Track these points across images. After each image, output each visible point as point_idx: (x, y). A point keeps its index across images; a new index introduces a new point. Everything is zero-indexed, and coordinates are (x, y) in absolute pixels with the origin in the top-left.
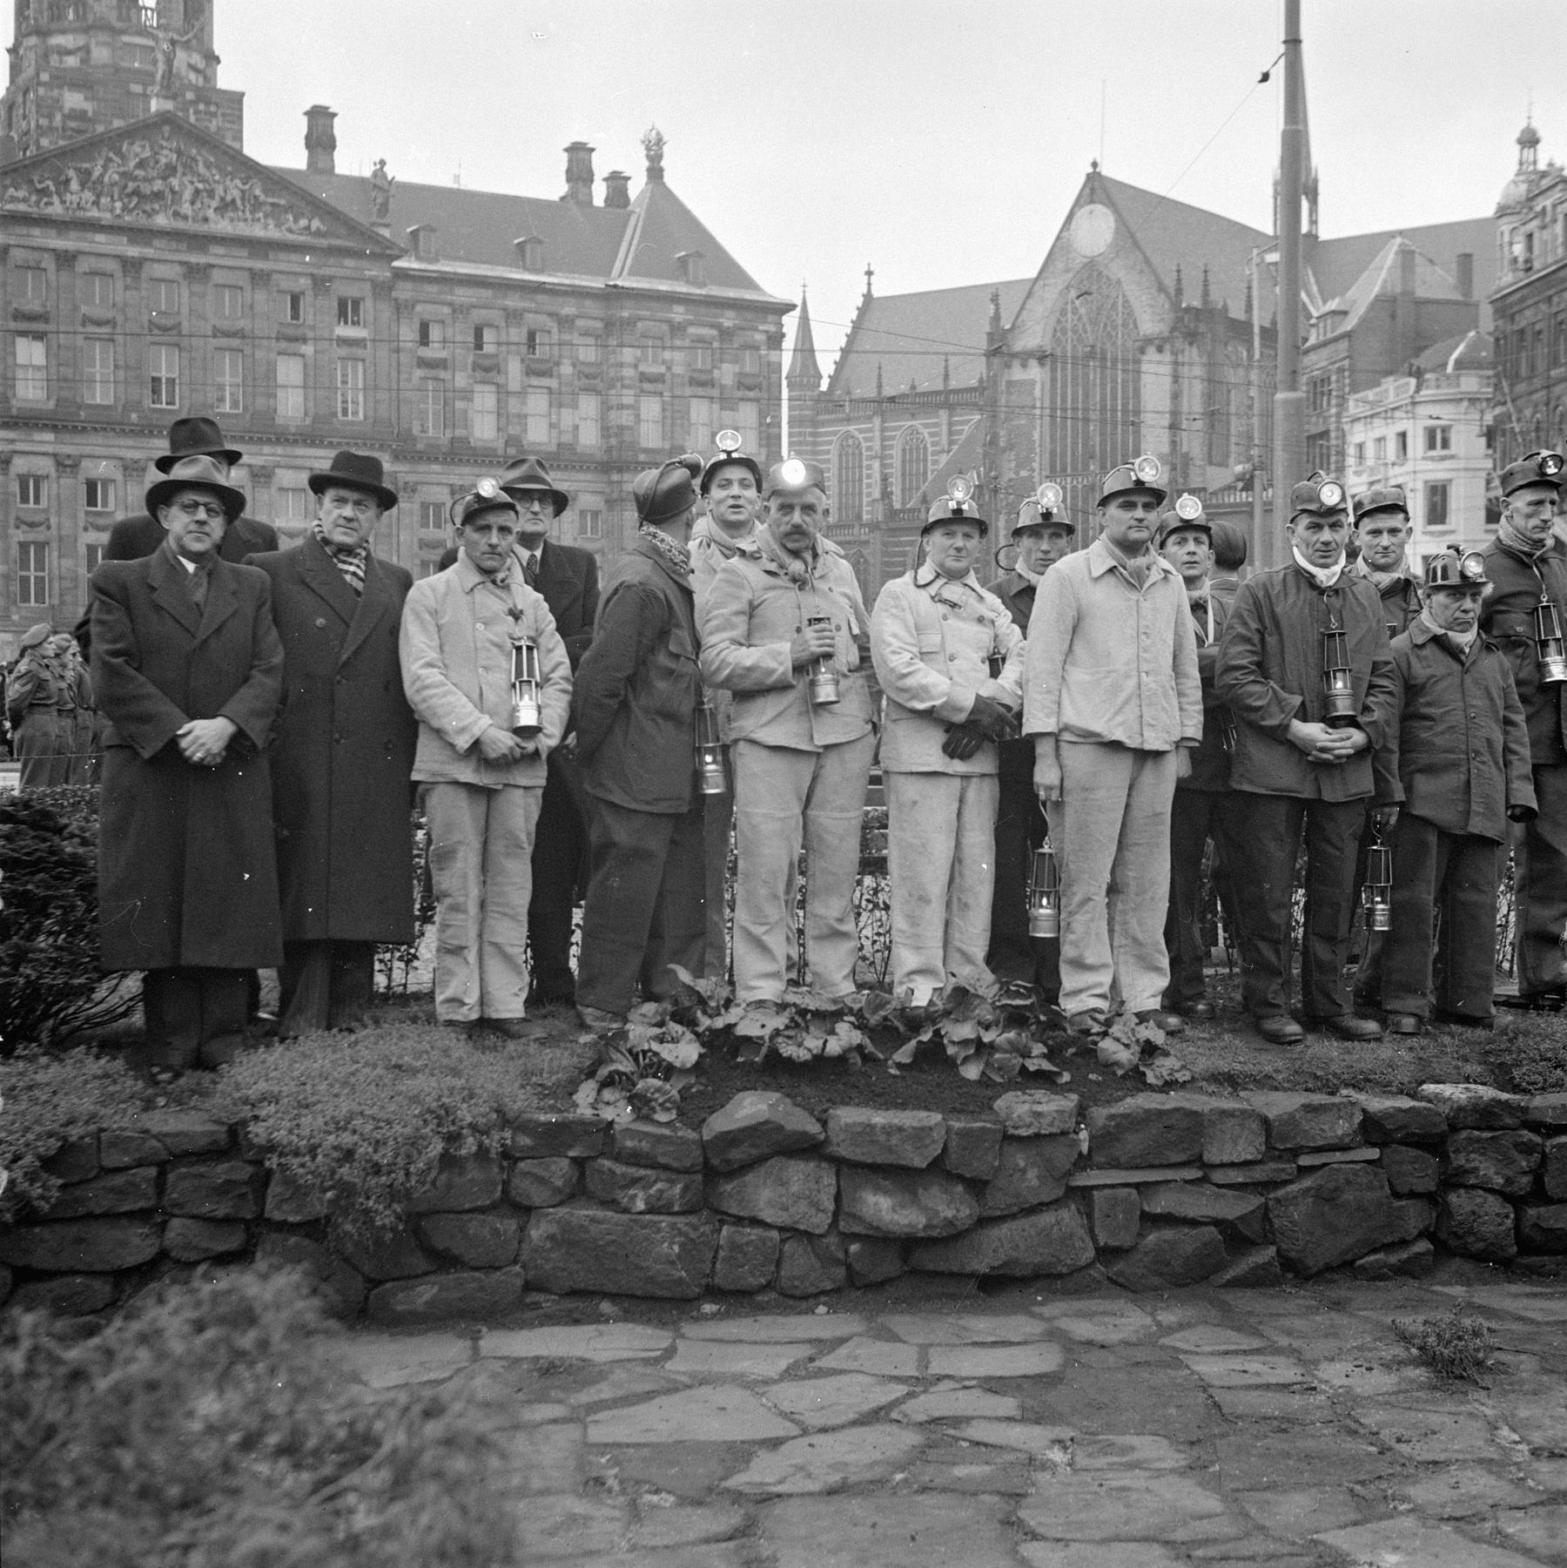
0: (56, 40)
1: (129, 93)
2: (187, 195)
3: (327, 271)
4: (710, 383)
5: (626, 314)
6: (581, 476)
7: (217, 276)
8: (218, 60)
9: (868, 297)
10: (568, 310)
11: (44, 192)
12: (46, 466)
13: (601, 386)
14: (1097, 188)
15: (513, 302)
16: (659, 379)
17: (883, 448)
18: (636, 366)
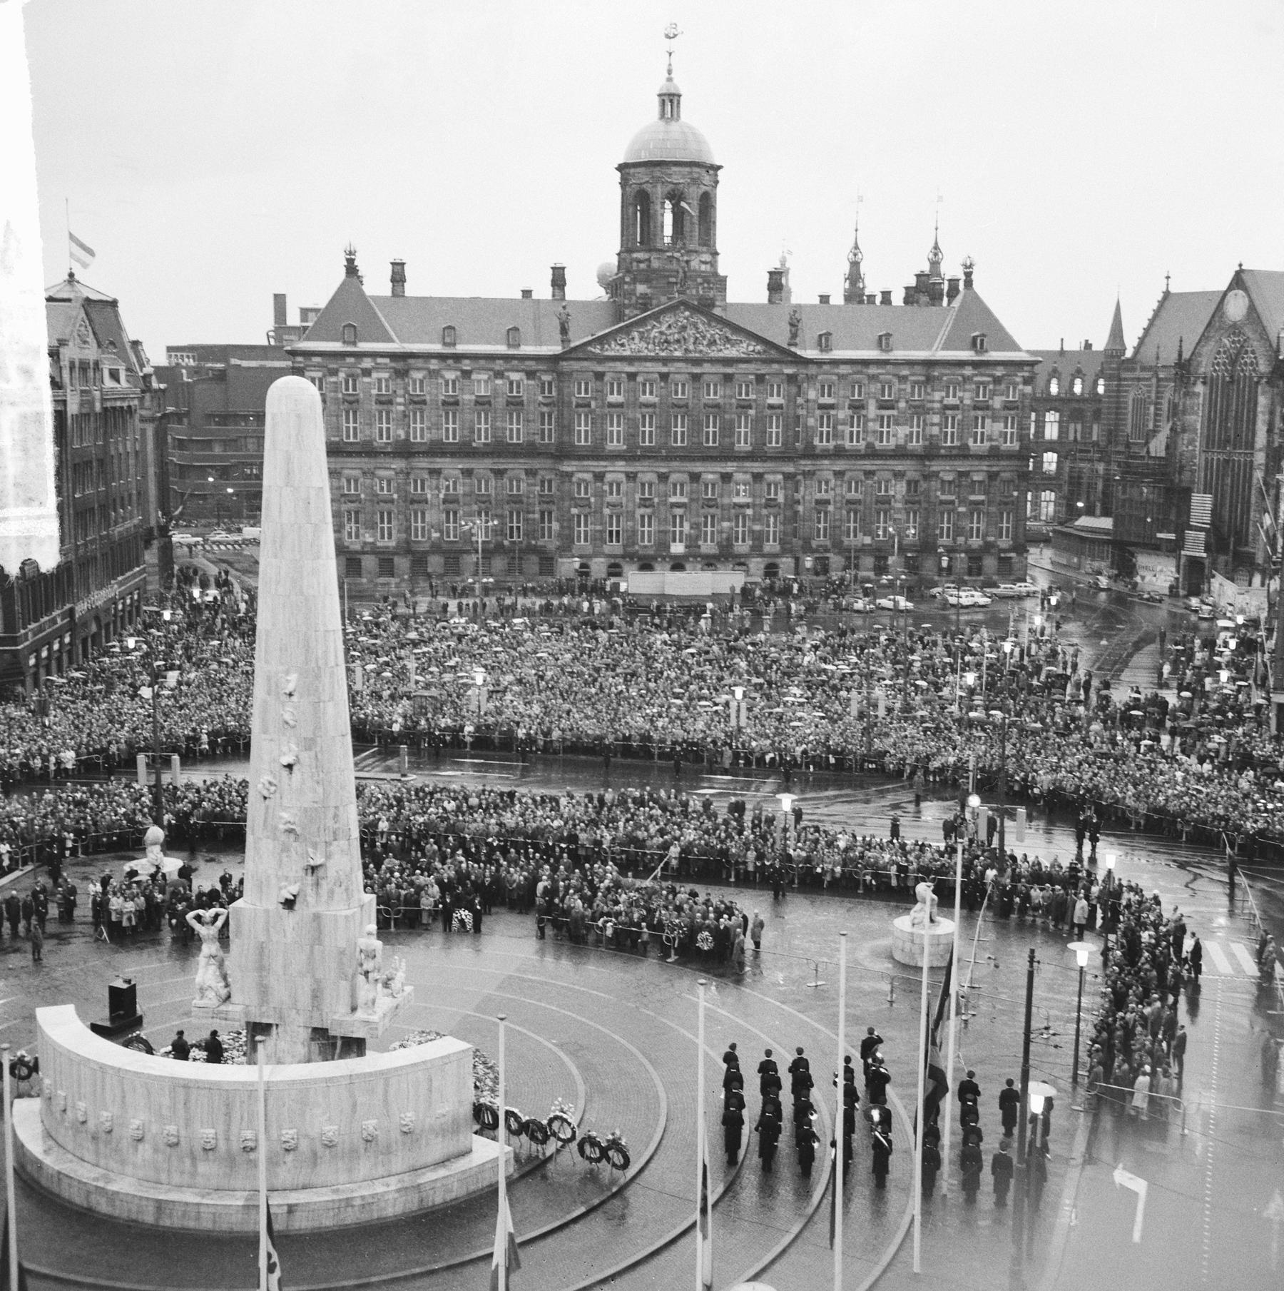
0: (635, 255)
1: (669, 283)
2: (692, 340)
3: (763, 372)
4: (987, 408)
6: (908, 462)
7: (705, 377)
8: (717, 254)
9: (1167, 294)
10: (905, 372)
11: (622, 345)
12: (622, 477)
15: (873, 370)
16: (955, 407)
17: (1157, 398)
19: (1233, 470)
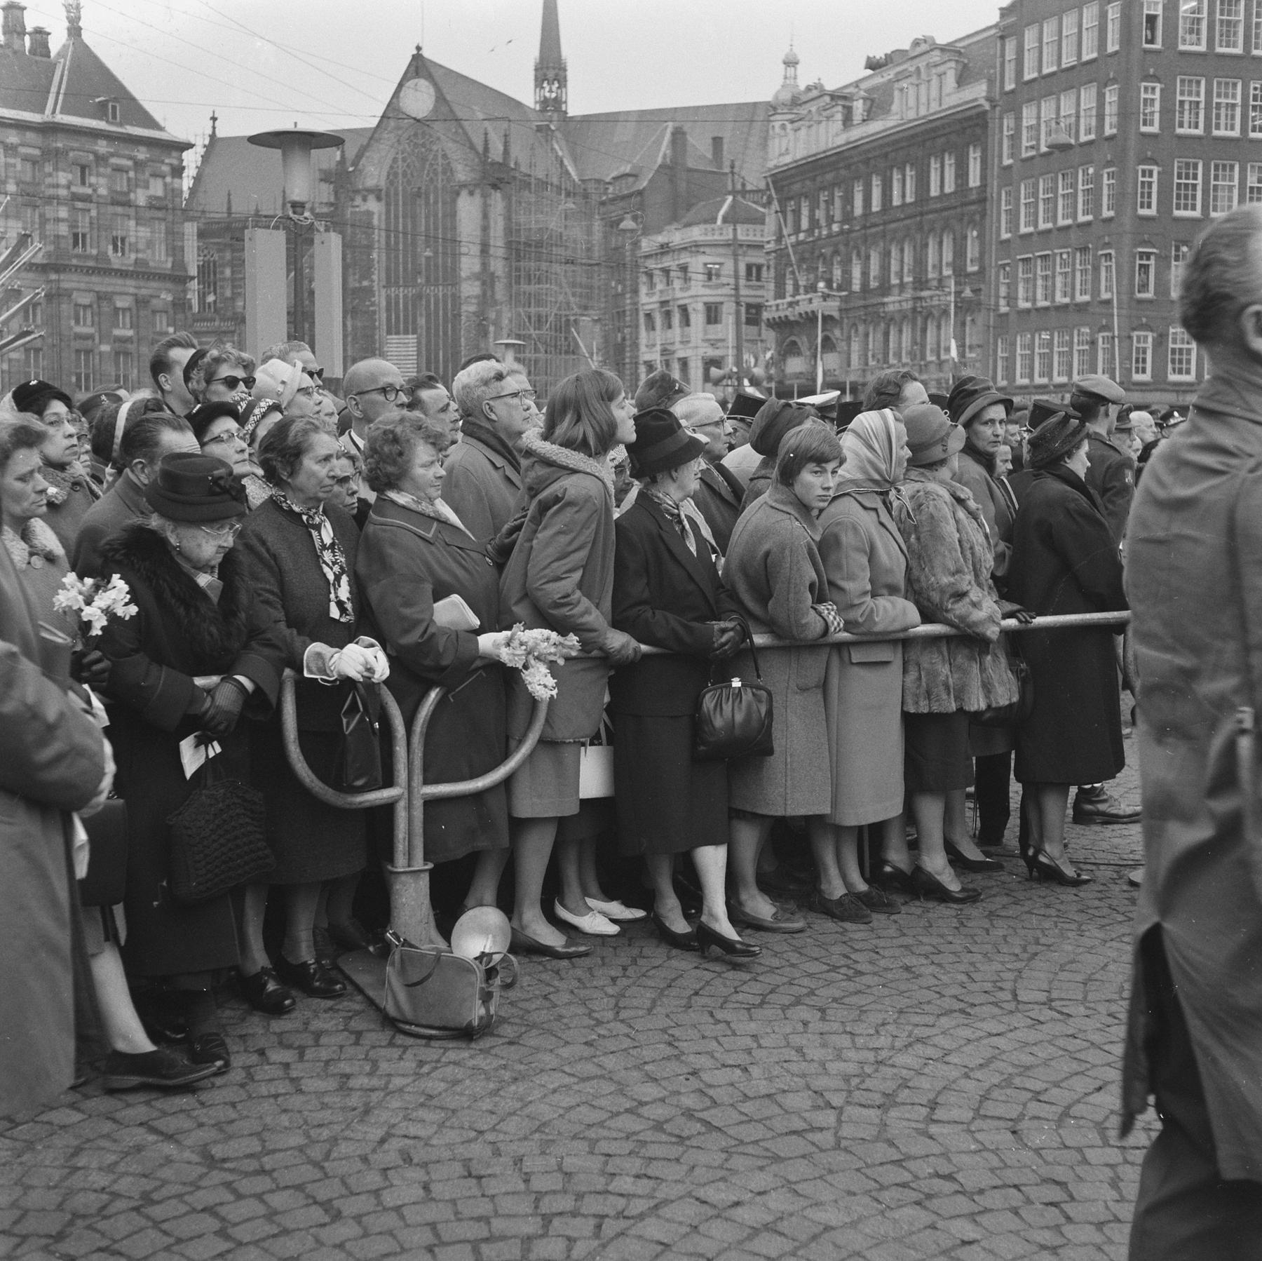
4: (128, 204)
5: (60, 145)
13: (39, 202)
14: (419, 66)
16: (86, 199)
18: (68, 187)
19: (428, 306)
